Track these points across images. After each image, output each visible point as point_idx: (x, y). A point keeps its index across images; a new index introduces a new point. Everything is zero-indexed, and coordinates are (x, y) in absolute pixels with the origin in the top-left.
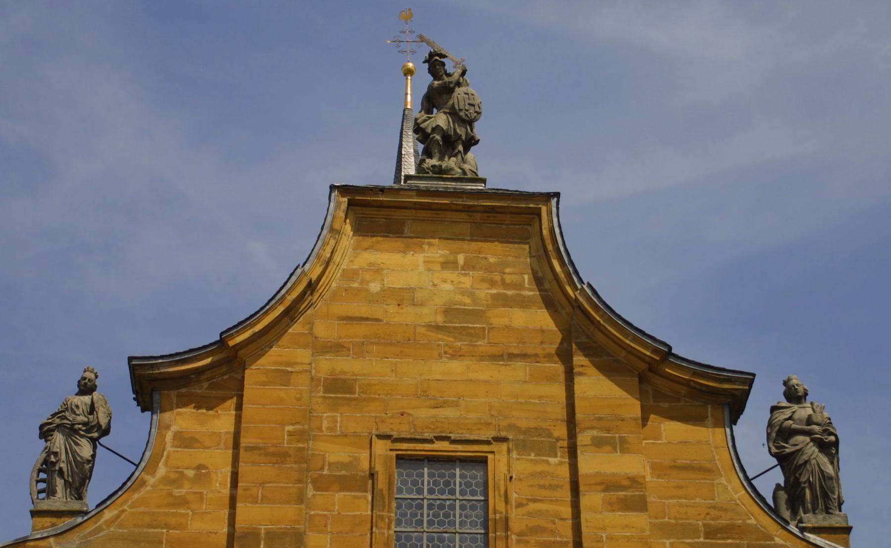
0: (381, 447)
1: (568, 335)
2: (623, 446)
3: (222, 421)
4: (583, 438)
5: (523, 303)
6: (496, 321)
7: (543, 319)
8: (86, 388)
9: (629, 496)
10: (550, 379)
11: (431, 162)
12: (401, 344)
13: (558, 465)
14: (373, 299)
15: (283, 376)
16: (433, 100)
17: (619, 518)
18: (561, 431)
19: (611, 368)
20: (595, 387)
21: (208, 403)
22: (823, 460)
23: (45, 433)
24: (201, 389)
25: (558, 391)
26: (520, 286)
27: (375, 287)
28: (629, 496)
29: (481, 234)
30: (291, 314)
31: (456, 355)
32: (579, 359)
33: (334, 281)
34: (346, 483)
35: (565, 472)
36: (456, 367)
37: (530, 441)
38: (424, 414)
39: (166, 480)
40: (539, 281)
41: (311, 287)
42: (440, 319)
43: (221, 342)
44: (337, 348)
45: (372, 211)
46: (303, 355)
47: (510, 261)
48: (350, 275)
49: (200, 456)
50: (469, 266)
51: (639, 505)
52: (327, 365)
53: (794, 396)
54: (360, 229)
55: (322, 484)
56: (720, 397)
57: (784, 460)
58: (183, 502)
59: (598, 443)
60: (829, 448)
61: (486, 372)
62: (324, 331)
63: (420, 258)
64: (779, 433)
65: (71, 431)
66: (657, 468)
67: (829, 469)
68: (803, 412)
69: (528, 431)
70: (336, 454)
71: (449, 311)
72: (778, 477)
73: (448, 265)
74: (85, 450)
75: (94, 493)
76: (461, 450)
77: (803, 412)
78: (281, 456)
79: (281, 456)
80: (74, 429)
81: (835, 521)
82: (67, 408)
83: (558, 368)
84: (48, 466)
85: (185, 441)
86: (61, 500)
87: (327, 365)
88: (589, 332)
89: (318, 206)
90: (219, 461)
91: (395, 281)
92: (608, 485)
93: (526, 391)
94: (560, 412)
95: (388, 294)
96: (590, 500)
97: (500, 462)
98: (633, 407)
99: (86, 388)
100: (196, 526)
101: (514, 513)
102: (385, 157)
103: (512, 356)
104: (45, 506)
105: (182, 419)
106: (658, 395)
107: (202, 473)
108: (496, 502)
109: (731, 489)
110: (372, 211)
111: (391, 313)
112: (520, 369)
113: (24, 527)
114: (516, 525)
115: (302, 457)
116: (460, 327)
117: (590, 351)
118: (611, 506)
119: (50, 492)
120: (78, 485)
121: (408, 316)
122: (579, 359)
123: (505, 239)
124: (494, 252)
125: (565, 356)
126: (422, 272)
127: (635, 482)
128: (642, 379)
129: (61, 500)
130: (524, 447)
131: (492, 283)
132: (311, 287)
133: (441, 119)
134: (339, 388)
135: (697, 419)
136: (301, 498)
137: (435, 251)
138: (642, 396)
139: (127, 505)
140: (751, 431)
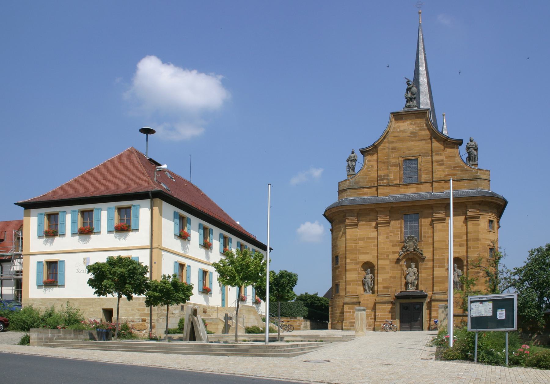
0: (400, 159)
1: (432, 134)
2: (440, 155)
3: (375, 157)
4: (434, 154)
5: (424, 130)
6: (419, 134)
7: (427, 132)
8: (353, 153)
9: (441, 163)
10: (429, 143)
11: (408, 104)
12: (403, 140)
13: (429, 158)
14: (398, 132)
15: (384, 149)
16: (408, 90)
17: (439, 167)
18: (430, 152)
19: (438, 141)
20: (436, 144)
21: (372, 154)
22: (475, 152)
23: (347, 161)
24: (371, 152)
25: (430, 145)
26: (423, 127)
27: (398, 130)
28: (441, 163)
29: (417, 117)
30: (384, 138)
31: (413, 141)
32: (433, 140)
33: (392, 130)
34: (395, 166)
35: (431, 160)
36: (412, 143)
37: (425, 155)
38: (407, 152)
39: (367, 168)
40: (427, 125)
41: (388, 132)
42: (410, 135)
43: (373, 145)
44: (393, 142)
45: (397, 116)
46: (387, 144)
47: (421, 122)
48: (394, 128)
49: (372, 163)
50: (415, 124)
51: (443, 164)
52: (391, 145)
53: (471, 141)
54: (396, 120)
55: (391, 166)
56: (458, 143)
57: (468, 153)
58: (369, 171)
59: (436, 155)
60: (476, 150)
61: (417, 143)
62: (390, 139)
63: (406, 123)
64: (468, 148)
65: (351, 161)
66: (446, 157)
67: (476, 154)
68: (473, 143)
69: (425, 153)
70: (393, 161)
71: (411, 133)
72: (467, 155)
73: (411, 124)
74: (354, 164)
75: (357, 170)
76: (413, 158)
77: (473, 143)
78: (384, 162)
79: (384, 162)
80: (352, 160)
81: (475, 163)
82: (350, 157)
83: (430, 141)
84: (348, 166)
85: (369, 161)
86: (351, 172)
87: (391, 145)
88: (436, 135)
89: (388, 117)
90: (375, 164)
91: (402, 129)
92: (437, 161)
93: (423, 146)
94: (430, 149)
95: (401, 131)
96: (435, 164)
97: (420, 159)
98: (442, 147)
99: (353, 153)
100: (372, 175)
101: (422, 168)
102: (400, 106)
103: (422, 140)
104: (349, 174)
105: (368, 157)
106: (447, 144)
107: (372, 166)
108: (419, 166)
109: (458, 160)
110: (397, 116)
111: (402, 135)
112: (424, 142)
113: (346, 177)
114: (422, 170)
115: (388, 162)
116: (413, 136)
117: (435, 138)
118: (438, 165)
119: (350, 171)
120: (353, 170)
121: (405, 135)
122: (433, 140)
123: (421, 118)
124: (419, 121)
125: (431, 139)
126: (407, 126)
127: (442, 160)
128: (444, 142)
129: (351, 172)
130: (424, 156)
131: (419, 127)
132: (388, 132)
133: (409, 95)
134: (393, 149)
135: (453, 148)
136: (388, 169)
137: (409, 122)
138: (444, 145)
139: (361, 173)
140: (463, 149)
